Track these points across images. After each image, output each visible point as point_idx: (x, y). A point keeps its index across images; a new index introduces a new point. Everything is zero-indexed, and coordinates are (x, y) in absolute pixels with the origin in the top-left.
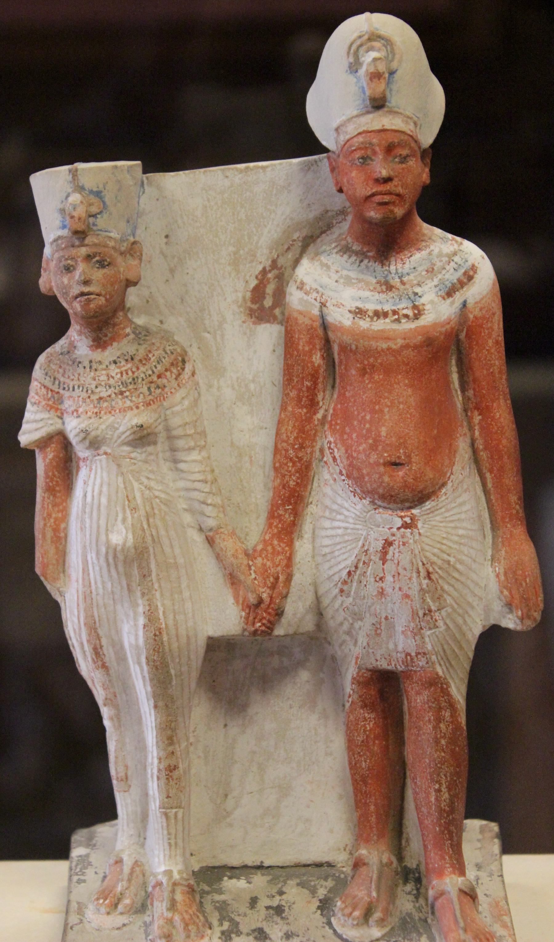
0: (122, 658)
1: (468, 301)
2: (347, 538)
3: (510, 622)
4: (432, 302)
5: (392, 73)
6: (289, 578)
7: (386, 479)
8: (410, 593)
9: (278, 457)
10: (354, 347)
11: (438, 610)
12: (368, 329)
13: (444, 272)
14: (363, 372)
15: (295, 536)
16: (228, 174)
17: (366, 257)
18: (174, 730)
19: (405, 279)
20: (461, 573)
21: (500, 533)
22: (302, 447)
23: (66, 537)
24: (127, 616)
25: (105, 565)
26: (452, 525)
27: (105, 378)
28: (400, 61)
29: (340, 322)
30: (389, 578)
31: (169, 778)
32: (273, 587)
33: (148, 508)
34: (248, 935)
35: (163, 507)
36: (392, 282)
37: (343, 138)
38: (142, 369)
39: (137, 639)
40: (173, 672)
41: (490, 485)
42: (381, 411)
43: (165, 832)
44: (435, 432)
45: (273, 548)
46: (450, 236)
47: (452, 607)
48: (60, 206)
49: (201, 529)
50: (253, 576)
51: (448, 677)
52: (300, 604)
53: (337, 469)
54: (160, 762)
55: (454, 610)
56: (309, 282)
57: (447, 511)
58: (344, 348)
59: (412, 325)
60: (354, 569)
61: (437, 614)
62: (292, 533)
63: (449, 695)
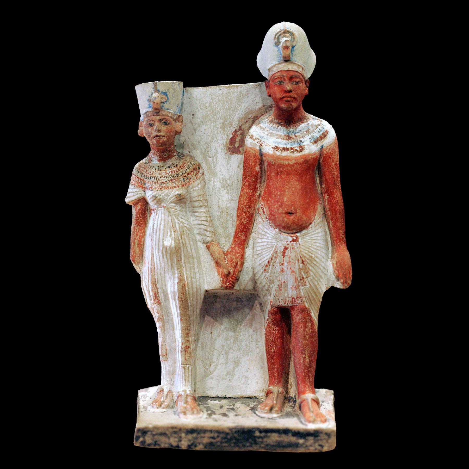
0: (166, 299)
1: (324, 146)
2: (268, 246)
3: (338, 285)
4: (308, 145)
5: (293, 47)
6: (242, 264)
7: (286, 219)
8: (295, 270)
9: (239, 211)
10: (273, 163)
11: (307, 278)
12: (280, 156)
13: (314, 132)
14: (277, 174)
15: (246, 246)
16: (221, 88)
17: (280, 125)
18: (189, 331)
19: (297, 135)
20: (317, 262)
21: (335, 247)
22: (250, 207)
23: (144, 244)
24: (170, 278)
25: (161, 255)
26: (314, 241)
27: (165, 174)
28: (297, 42)
29: (268, 152)
30: (286, 264)
31: (186, 351)
32: (235, 267)
33: (181, 231)
34: (219, 414)
35: (188, 231)
36: (291, 136)
37: (271, 73)
38: (181, 170)
39: (174, 289)
40: (189, 304)
41: (331, 226)
42: (285, 191)
43: (184, 375)
44: (308, 201)
45: (236, 251)
46: (317, 118)
47: (313, 277)
48: (149, 98)
49: (204, 243)
50: (227, 262)
51: (310, 308)
52: (247, 276)
53: (265, 216)
54: (182, 345)
55: (314, 278)
56: (255, 135)
57: (312, 235)
58: (269, 164)
59: (299, 154)
60: (270, 260)
61: (306, 279)
62: (244, 244)
63: (310, 316)
